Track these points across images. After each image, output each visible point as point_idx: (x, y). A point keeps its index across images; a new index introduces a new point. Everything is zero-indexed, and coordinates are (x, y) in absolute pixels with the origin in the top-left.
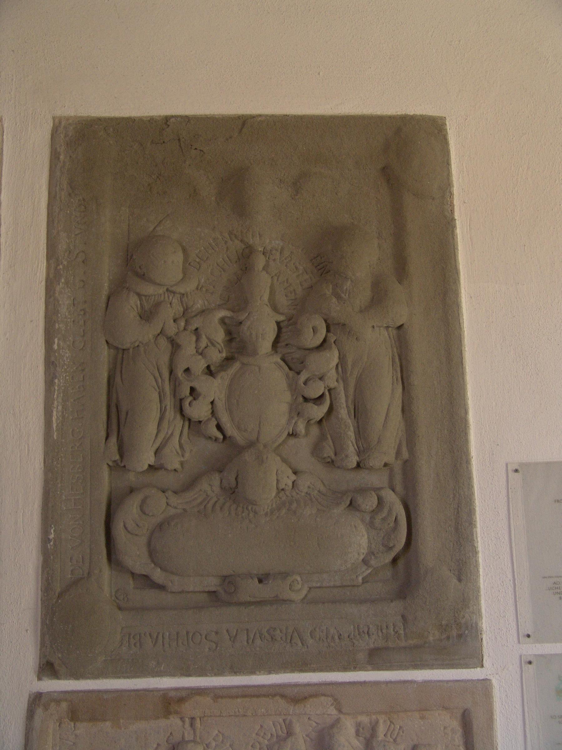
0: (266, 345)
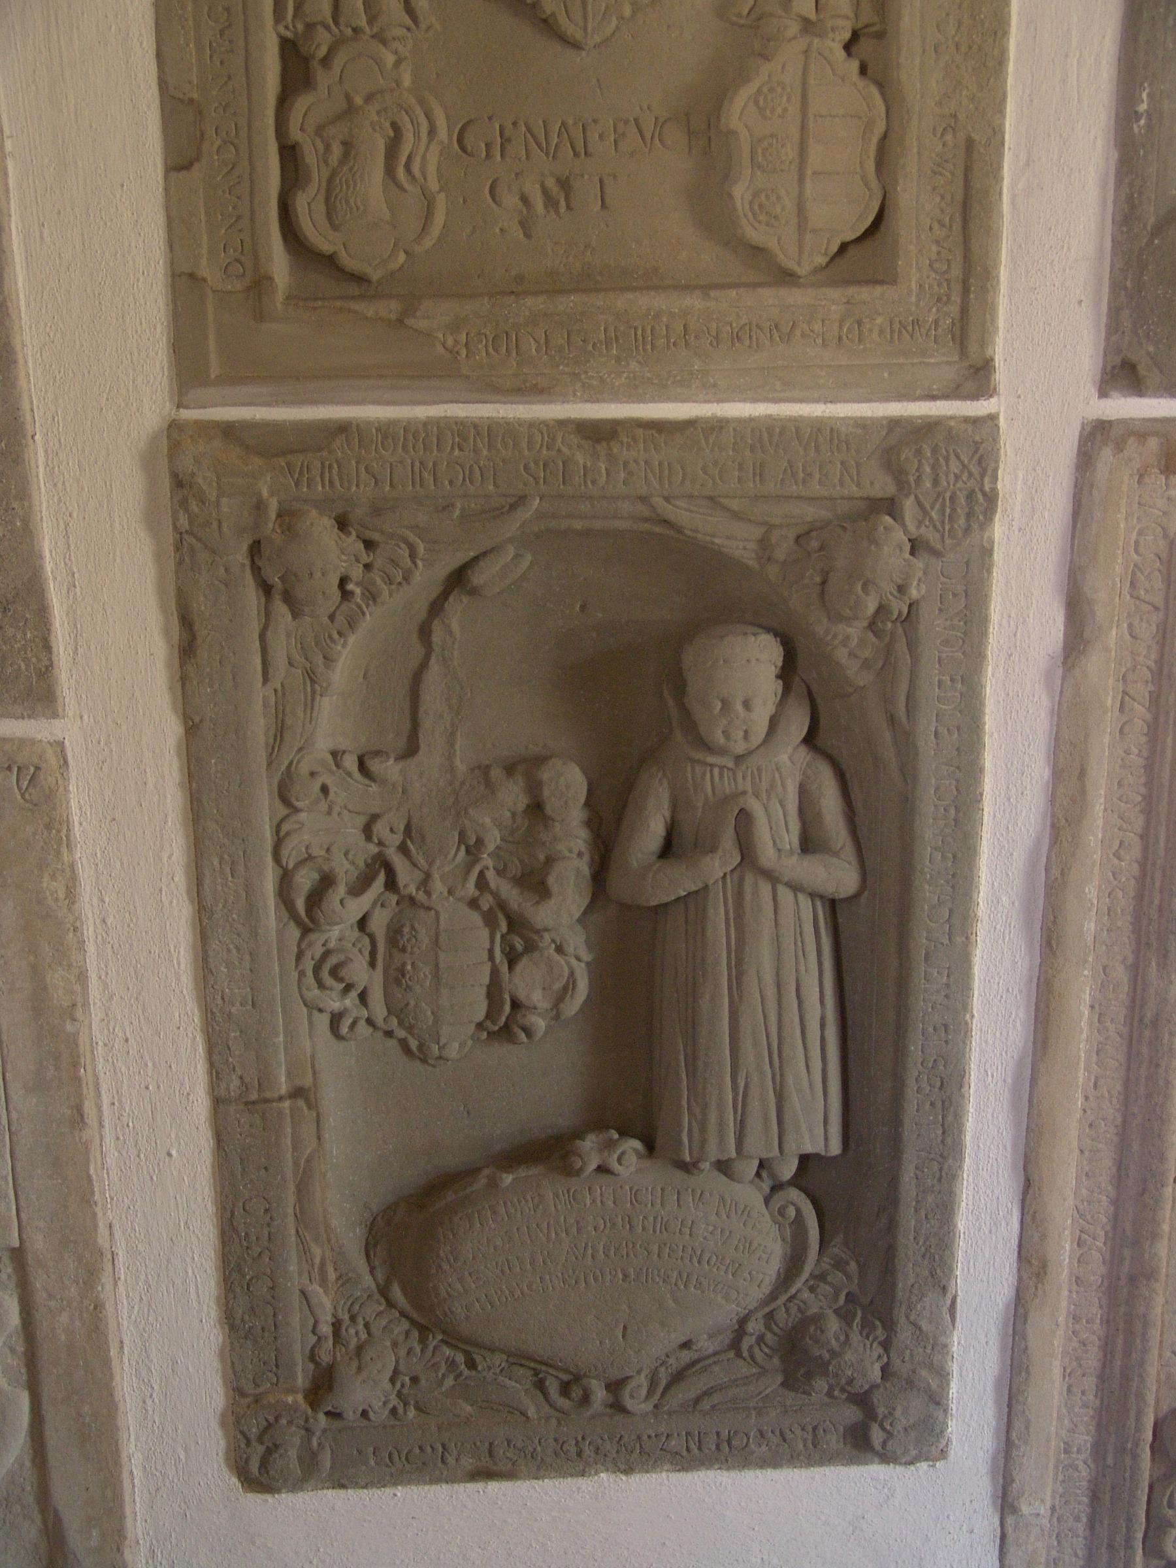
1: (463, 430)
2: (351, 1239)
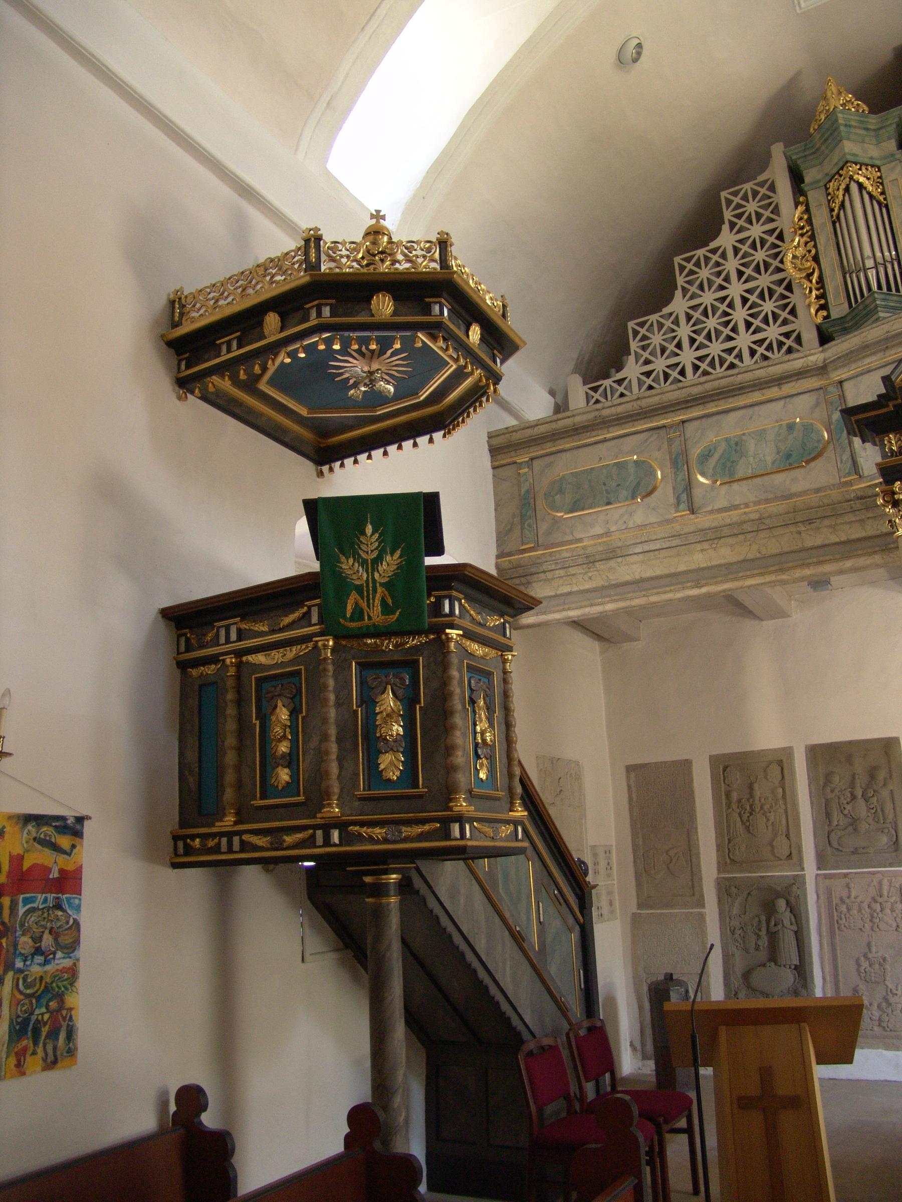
0: (860, 796)
2: (739, 976)
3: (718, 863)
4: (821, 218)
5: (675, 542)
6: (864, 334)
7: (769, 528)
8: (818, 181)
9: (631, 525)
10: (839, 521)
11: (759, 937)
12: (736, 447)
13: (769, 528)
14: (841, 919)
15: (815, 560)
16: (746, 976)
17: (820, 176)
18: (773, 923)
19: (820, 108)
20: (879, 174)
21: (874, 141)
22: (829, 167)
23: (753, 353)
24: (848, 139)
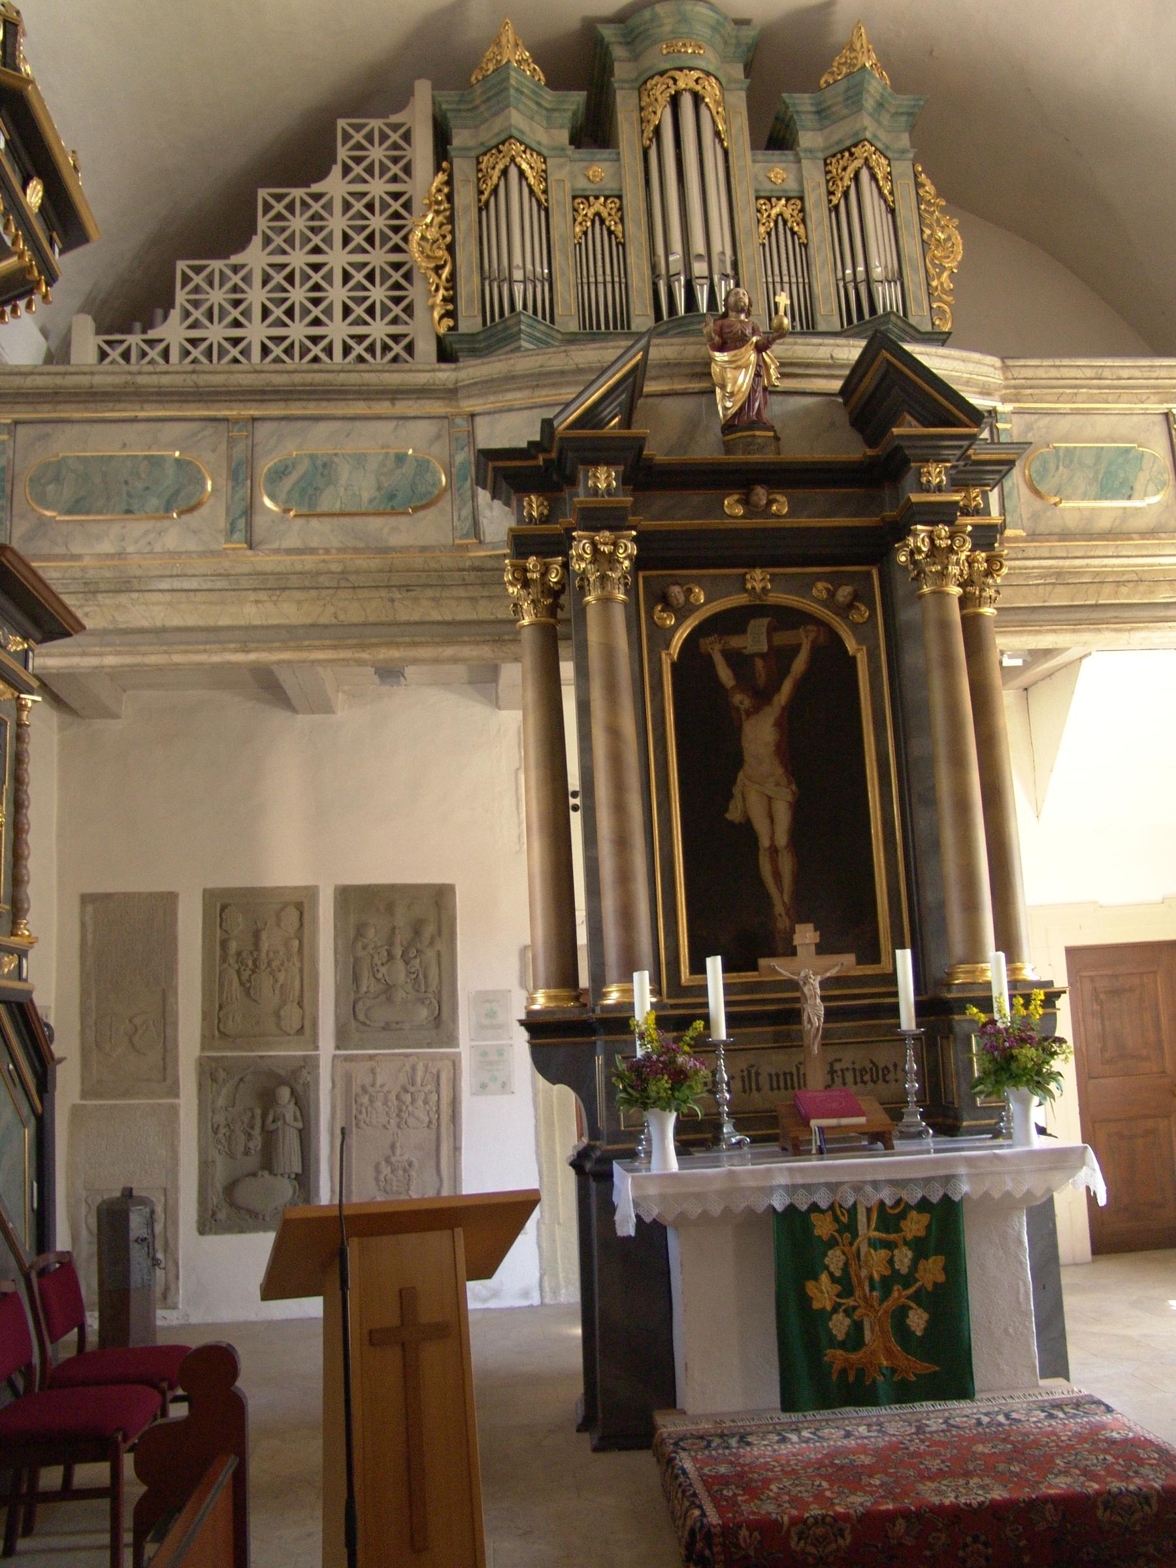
0: (399, 957)
1: (242, 1057)
2: (220, 1190)
3: (203, 1036)
4: (465, 197)
5: (220, 584)
6: (512, 361)
7: (354, 588)
8: (469, 149)
9: (158, 548)
10: (446, 593)
11: (250, 1136)
12: (324, 469)
13: (354, 588)
14: (361, 1112)
15: (407, 639)
16: (230, 1189)
17: (471, 143)
18: (271, 1118)
19: (489, 54)
20: (544, 167)
21: (544, 123)
22: (488, 134)
23: (347, 350)
24: (517, 109)
